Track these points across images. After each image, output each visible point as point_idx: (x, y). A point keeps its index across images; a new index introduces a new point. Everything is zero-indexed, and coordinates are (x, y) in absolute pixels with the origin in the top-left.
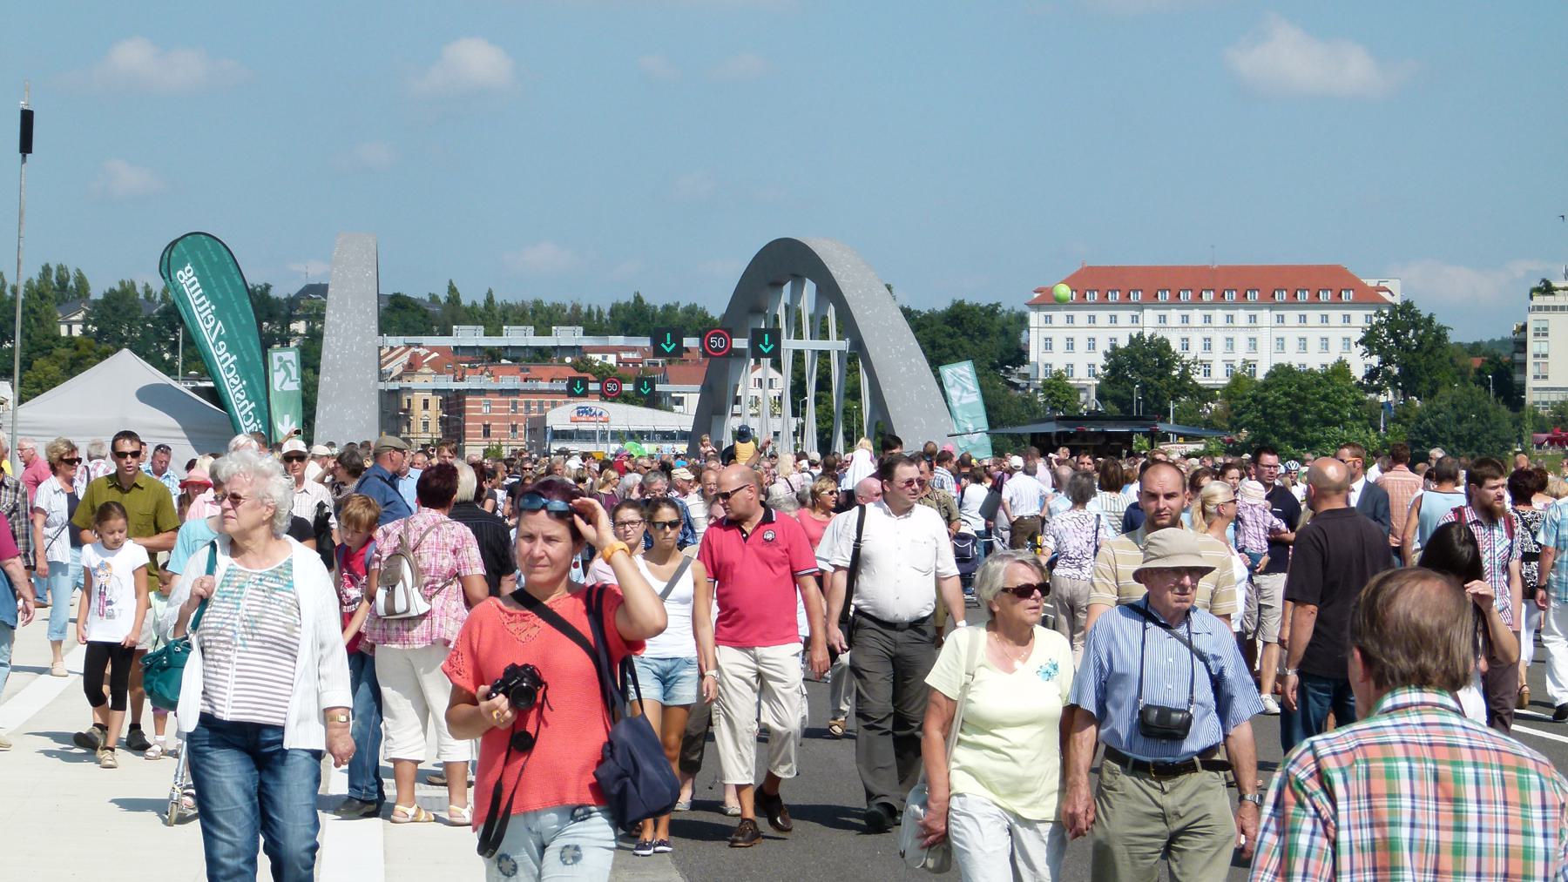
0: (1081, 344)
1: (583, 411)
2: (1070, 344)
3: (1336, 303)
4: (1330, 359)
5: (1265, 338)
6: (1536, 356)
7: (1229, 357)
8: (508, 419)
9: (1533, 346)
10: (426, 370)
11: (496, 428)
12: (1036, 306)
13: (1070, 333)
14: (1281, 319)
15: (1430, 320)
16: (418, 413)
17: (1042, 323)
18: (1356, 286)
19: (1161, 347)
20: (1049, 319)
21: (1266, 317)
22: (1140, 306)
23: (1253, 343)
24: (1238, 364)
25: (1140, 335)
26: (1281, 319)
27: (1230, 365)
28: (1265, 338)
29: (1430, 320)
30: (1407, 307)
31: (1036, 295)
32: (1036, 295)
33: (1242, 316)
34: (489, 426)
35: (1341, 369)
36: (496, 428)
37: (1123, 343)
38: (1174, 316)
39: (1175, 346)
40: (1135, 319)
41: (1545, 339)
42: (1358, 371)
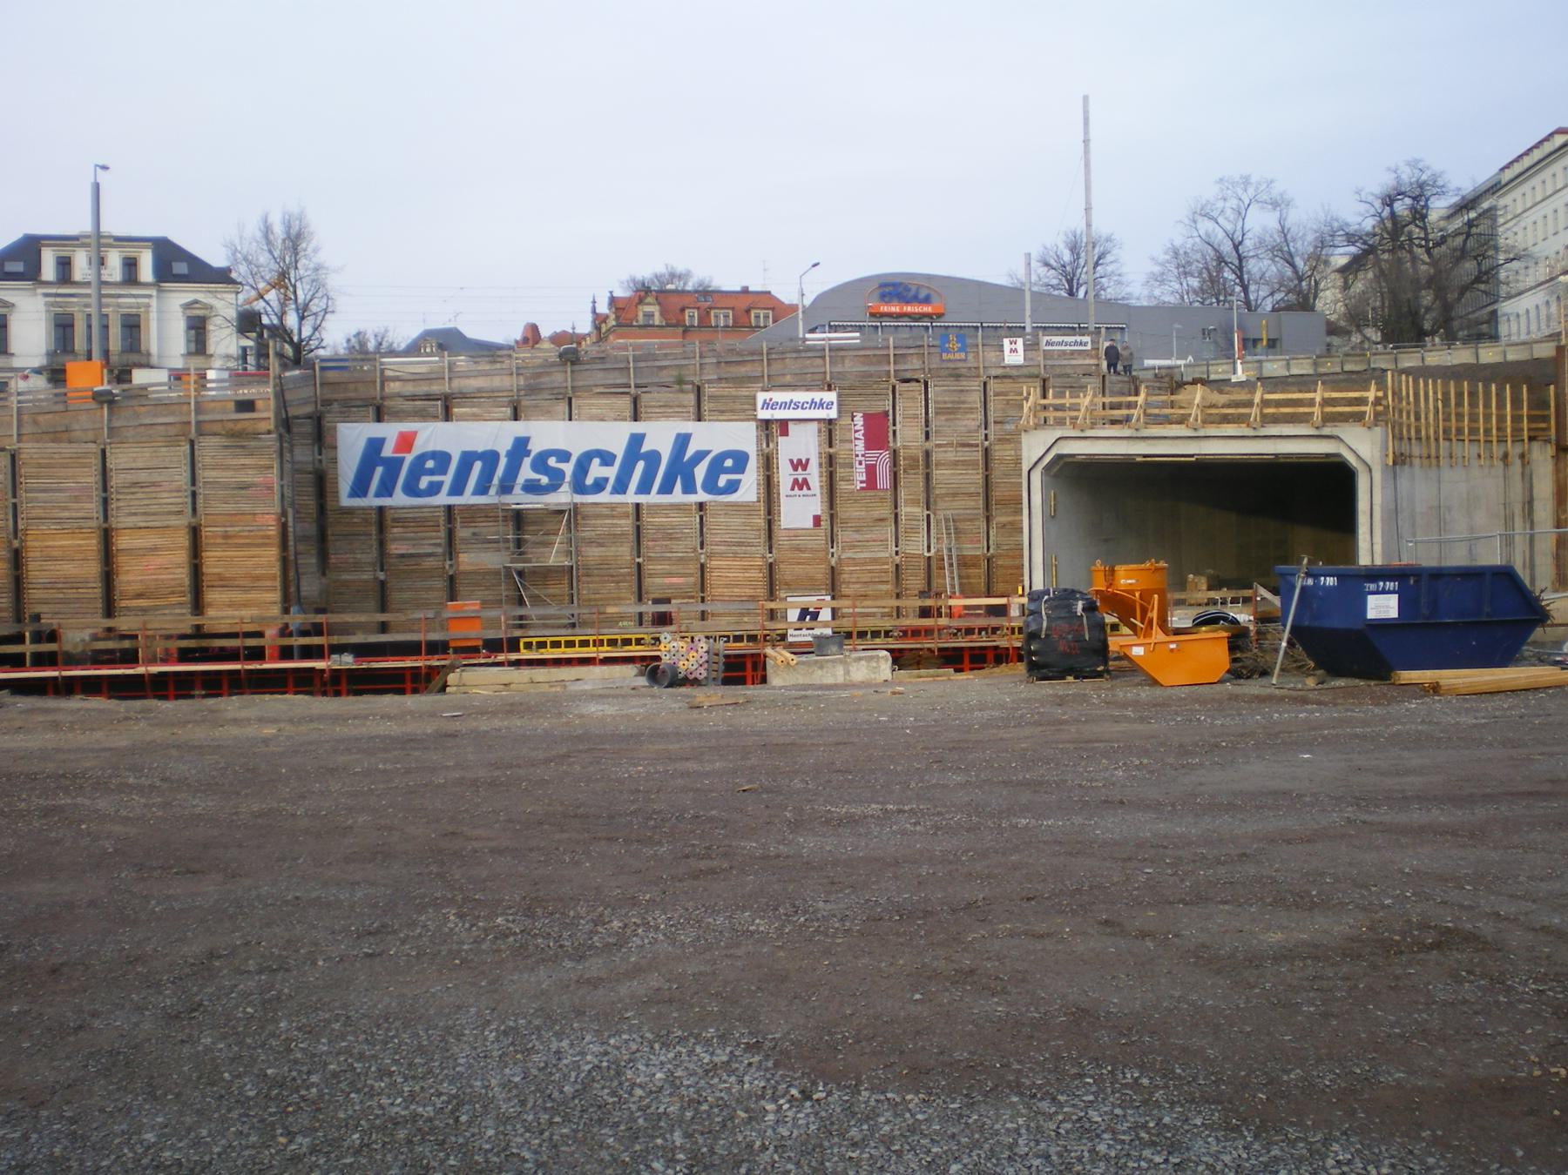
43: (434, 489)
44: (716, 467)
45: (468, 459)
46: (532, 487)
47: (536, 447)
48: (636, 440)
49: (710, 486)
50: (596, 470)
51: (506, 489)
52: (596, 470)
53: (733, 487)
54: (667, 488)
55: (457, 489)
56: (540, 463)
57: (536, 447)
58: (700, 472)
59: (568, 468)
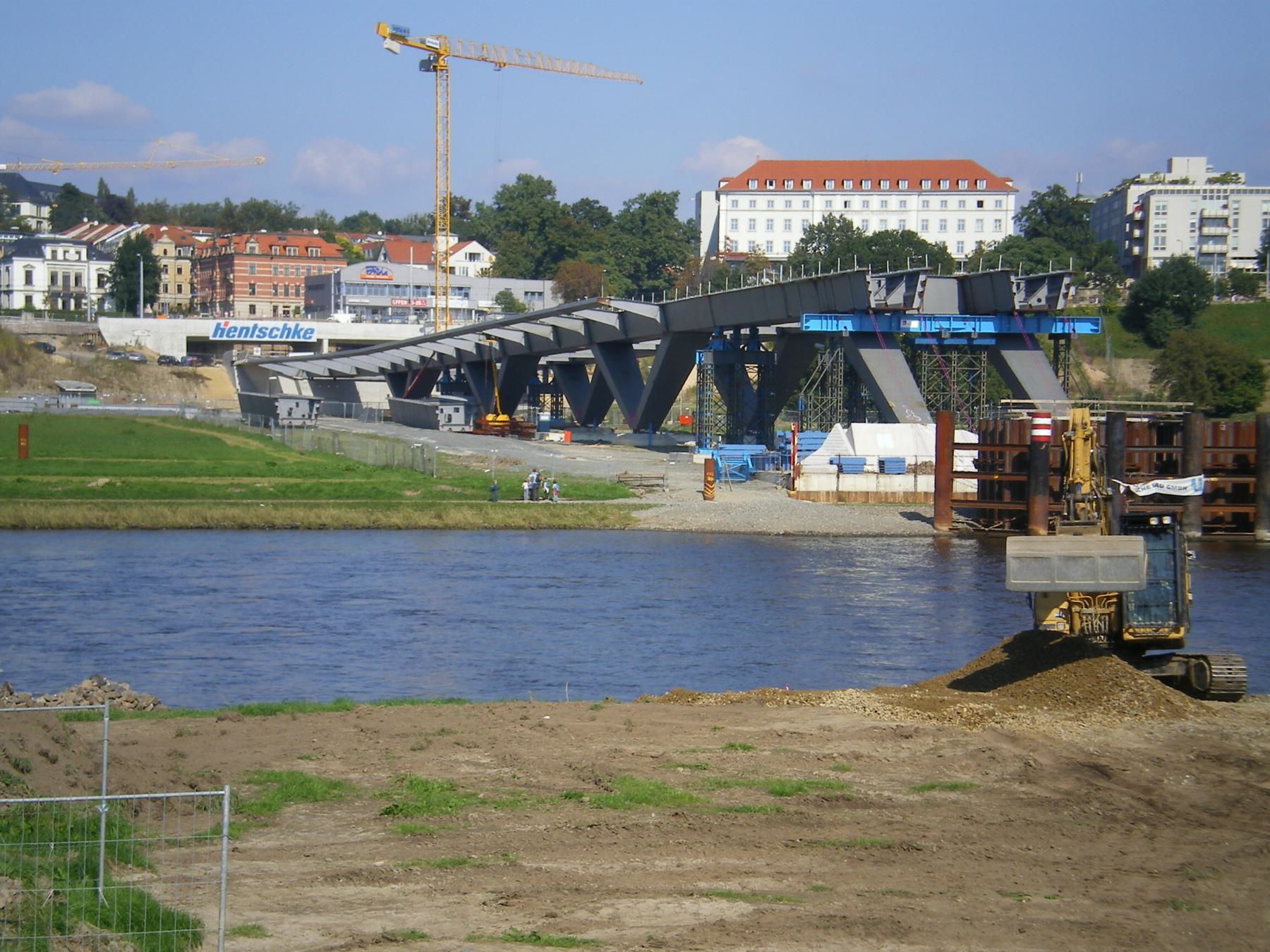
0: (779, 225)
1: (373, 270)
2: (752, 225)
3: (973, 188)
8: (270, 279)
9: (1154, 221)
11: (260, 287)
12: (727, 191)
13: (752, 215)
14: (926, 203)
17: (730, 207)
18: (986, 175)
20: (735, 203)
22: (811, 192)
26: (926, 203)
31: (723, 184)
32: (723, 184)
33: (894, 200)
34: (254, 285)
36: (260, 287)
38: (838, 201)
41: (1164, 216)
43: (233, 336)
44: (306, 332)
45: (242, 329)
46: (258, 336)
47: (259, 326)
48: (285, 325)
49: (304, 337)
50: (275, 332)
51: (252, 336)
52: (275, 332)
53: (310, 338)
54: (293, 337)
55: (239, 336)
56: (260, 330)
57: (259, 326)
58: (302, 333)
59: (268, 332)
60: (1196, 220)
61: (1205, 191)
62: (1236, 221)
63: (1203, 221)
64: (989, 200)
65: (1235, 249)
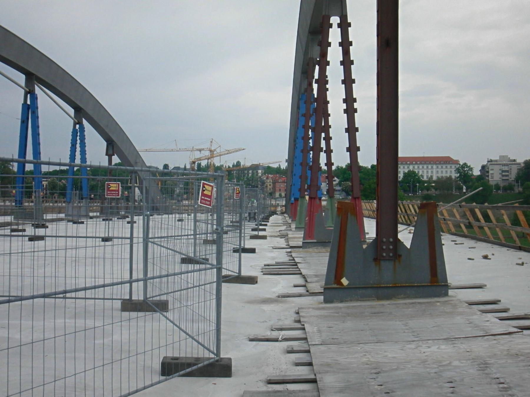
4: (448, 175)
5: (434, 171)
6: (491, 174)
7: (427, 175)
10: (270, 179)
15: (470, 166)
16: (269, 187)
19: (414, 172)
21: (435, 167)
22: (409, 164)
23: (432, 172)
24: (430, 176)
25: (410, 170)
26: (438, 167)
27: (427, 176)
28: (434, 171)
29: (470, 166)
30: (465, 164)
35: (451, 176)
37: (406, 171)
38: (416, 167)
39: (417, 172)
40: (408, 167)
42: (453, 177)
60: (500, 172)
61: (503, 164)
62: (511, 172)
63: (503, 171)
64: (453, 166)
65: (511, 178)
